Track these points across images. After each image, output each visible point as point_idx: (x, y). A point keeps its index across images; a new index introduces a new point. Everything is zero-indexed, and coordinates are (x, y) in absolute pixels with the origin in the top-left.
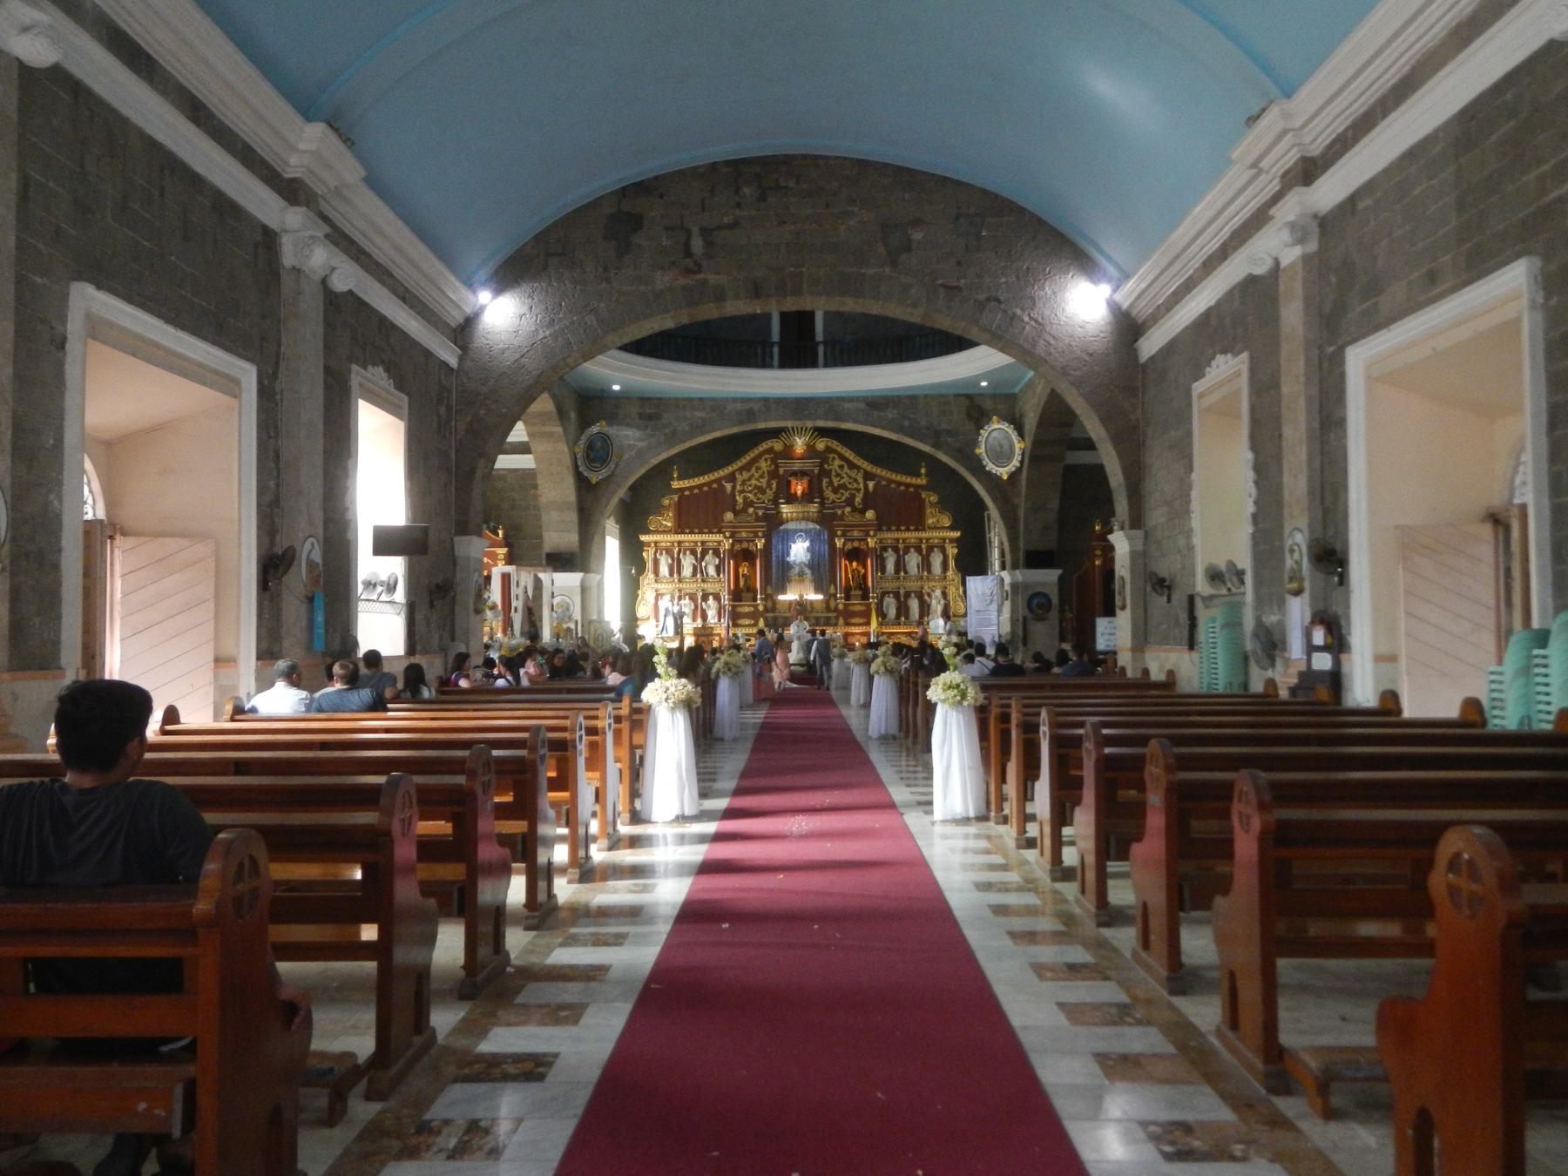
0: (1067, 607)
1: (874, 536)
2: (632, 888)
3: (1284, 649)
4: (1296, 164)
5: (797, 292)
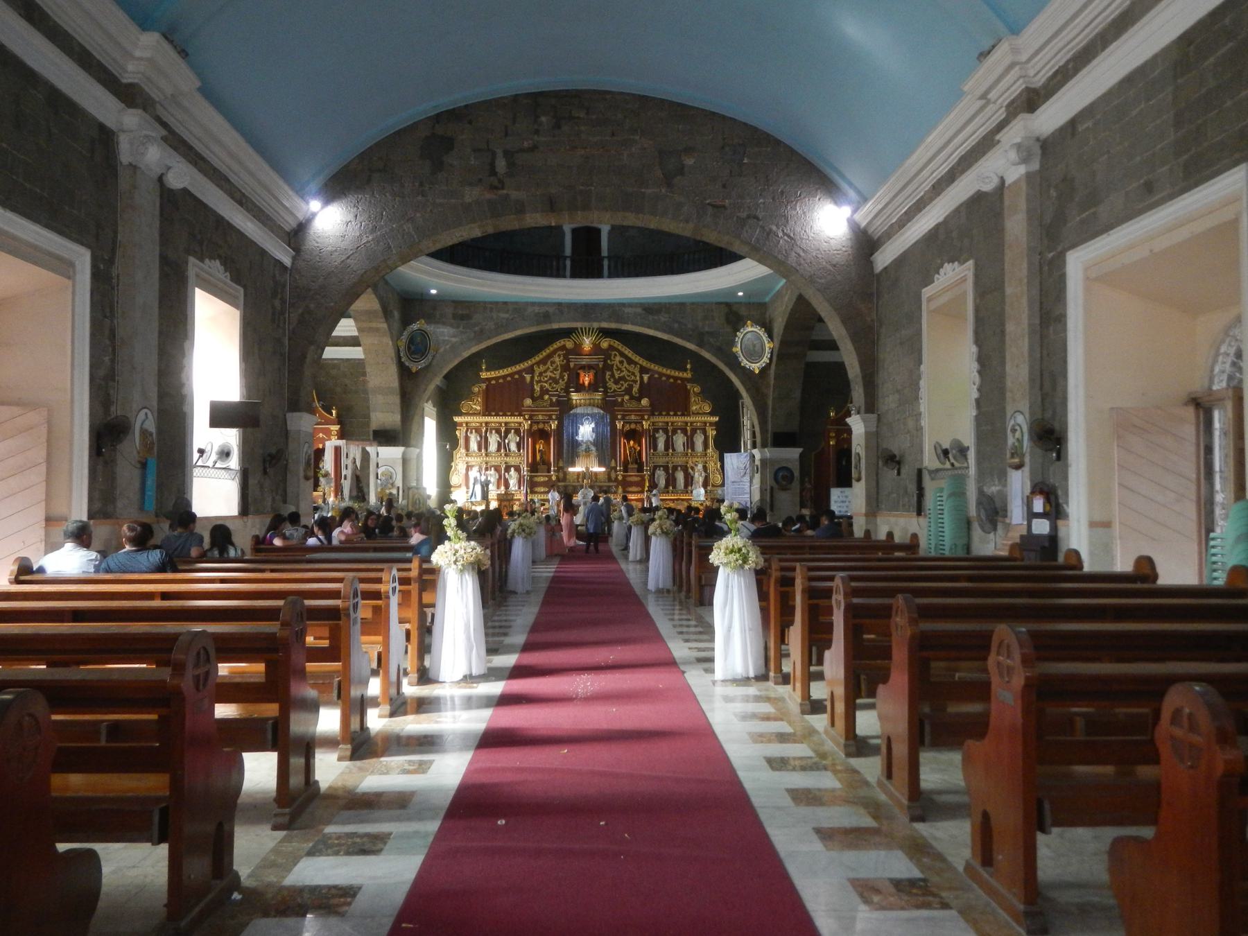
0: (807, 479)
1: (648, 419)
2: (407, 767)
3: (1006, 516)
4: (1021, 94)
5: (586, 207)
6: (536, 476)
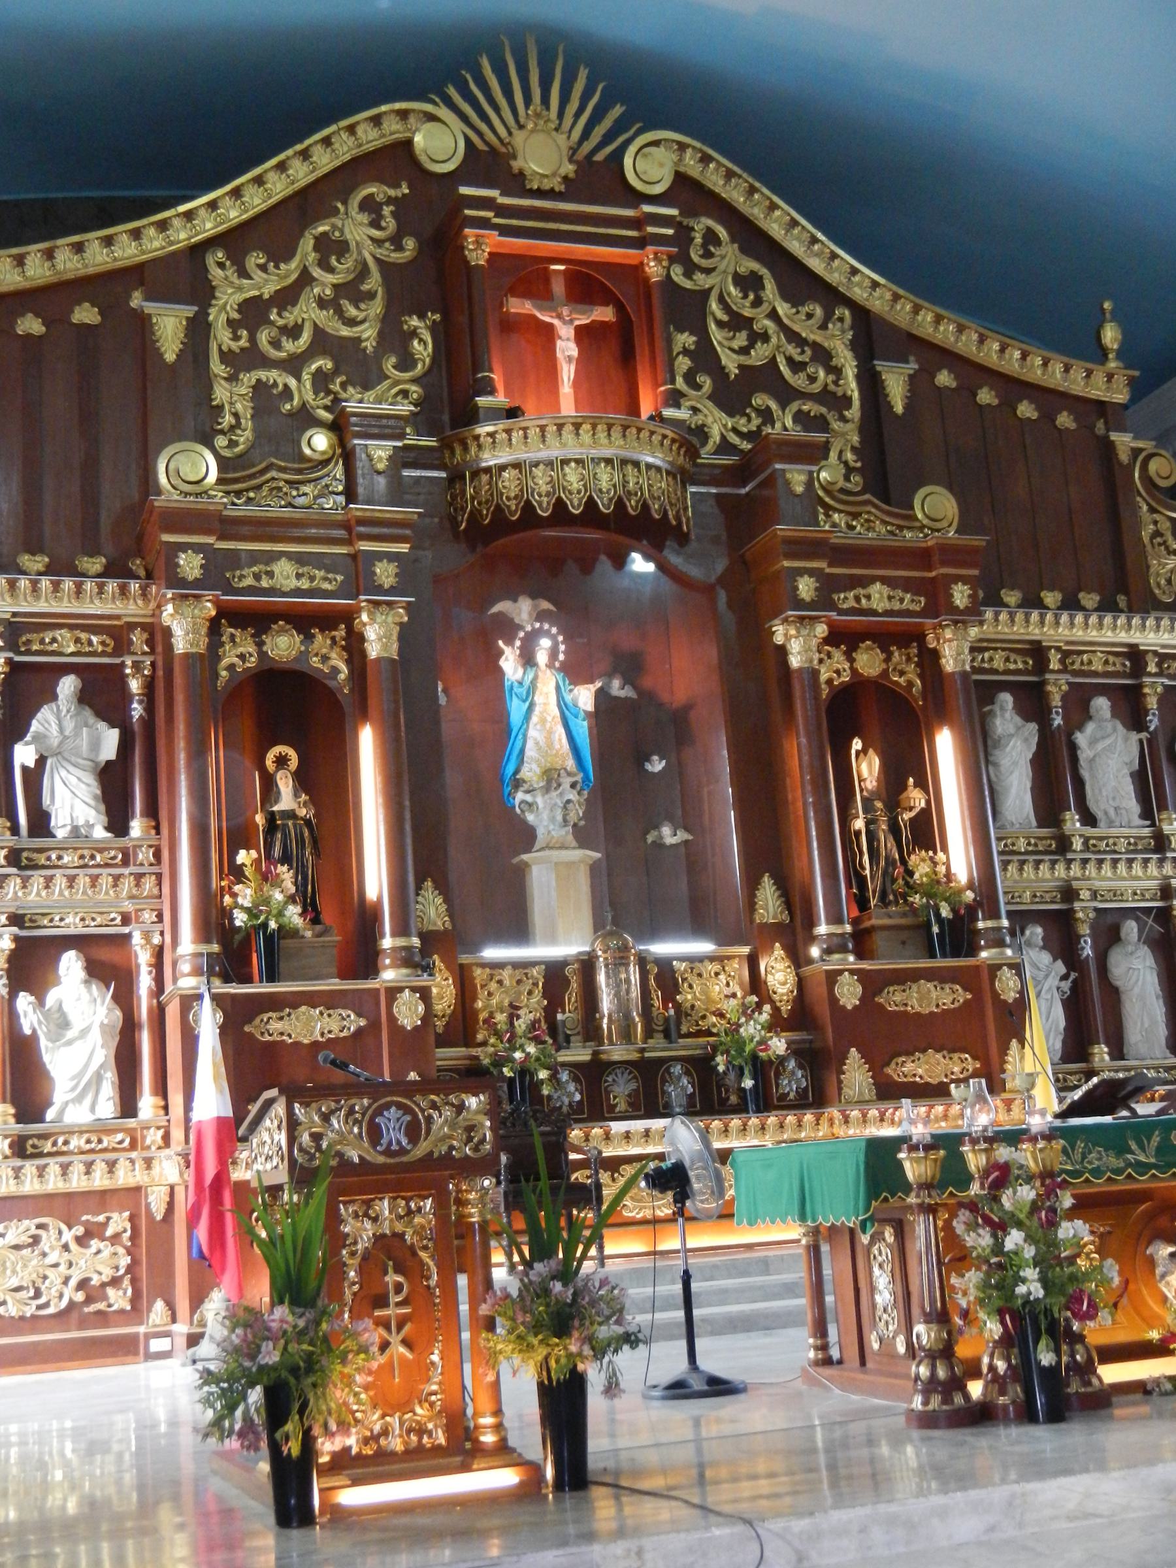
1: (973, 612)
6: (275, 1003)
